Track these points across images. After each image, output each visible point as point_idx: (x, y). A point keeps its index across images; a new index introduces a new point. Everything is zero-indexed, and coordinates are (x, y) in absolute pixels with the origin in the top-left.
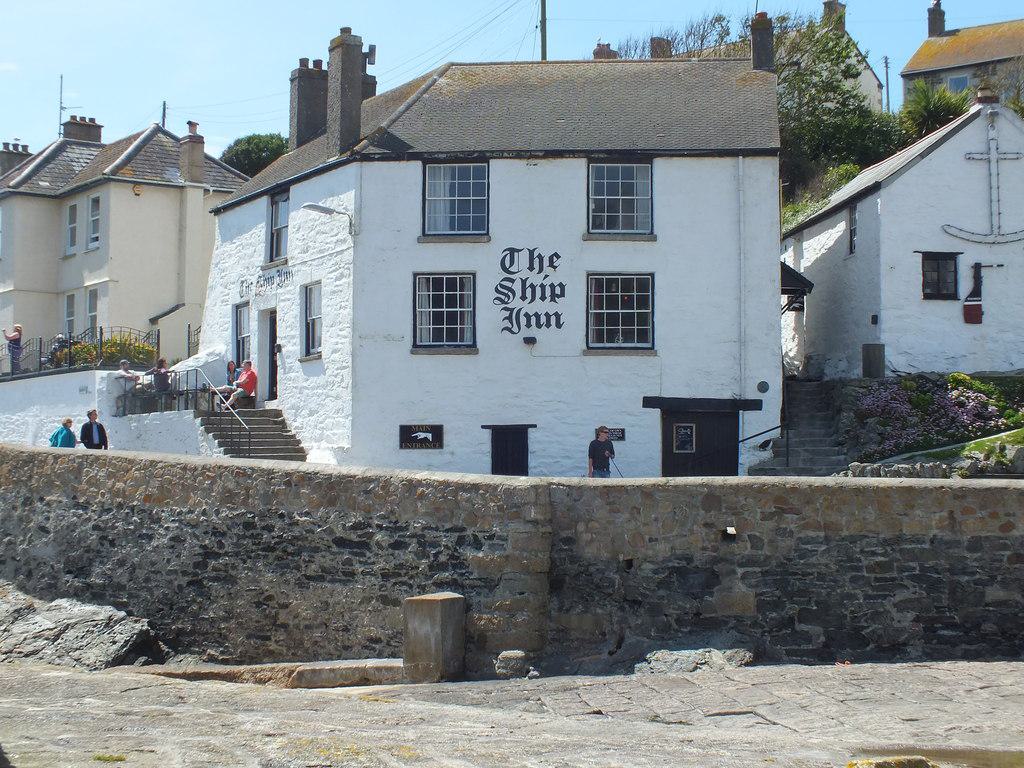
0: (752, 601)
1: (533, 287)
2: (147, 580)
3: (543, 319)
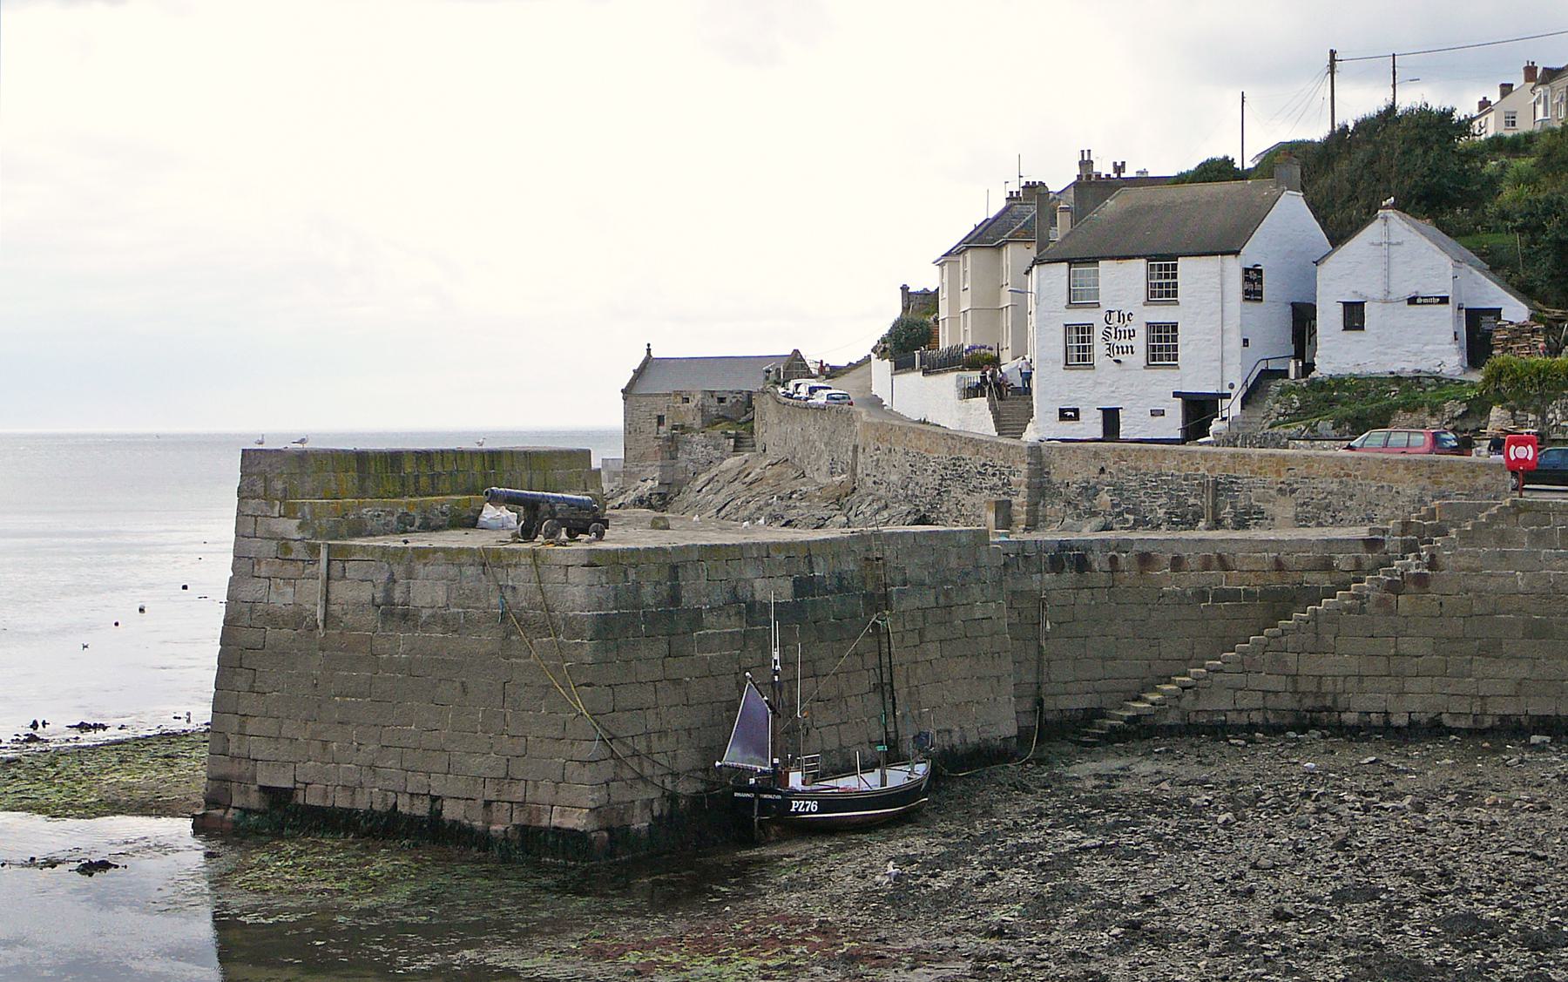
3: (1125, 349)
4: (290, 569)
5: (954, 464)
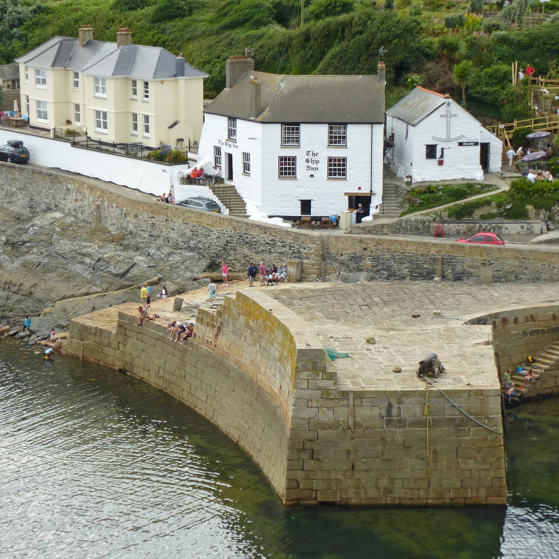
0: (371, 265)
2: (209, 247)
4: (330, 403)
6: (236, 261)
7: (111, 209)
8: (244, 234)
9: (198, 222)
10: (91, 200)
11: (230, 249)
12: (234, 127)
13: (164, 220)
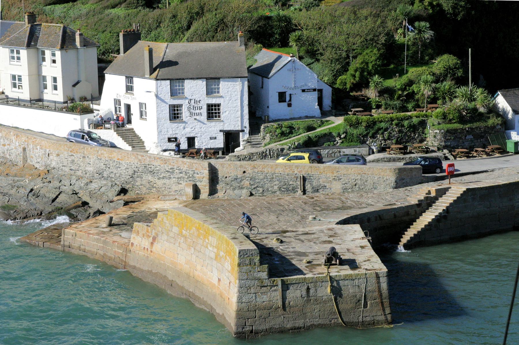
1: (195, 107)
5: (145, 167)
6: (142, 186)
7: (35, 151)
8: (149, 165)
9: (109, 157)
10: (17, 144)
11: (138, 177)
12: (131, 83)
13: (81, 157)
